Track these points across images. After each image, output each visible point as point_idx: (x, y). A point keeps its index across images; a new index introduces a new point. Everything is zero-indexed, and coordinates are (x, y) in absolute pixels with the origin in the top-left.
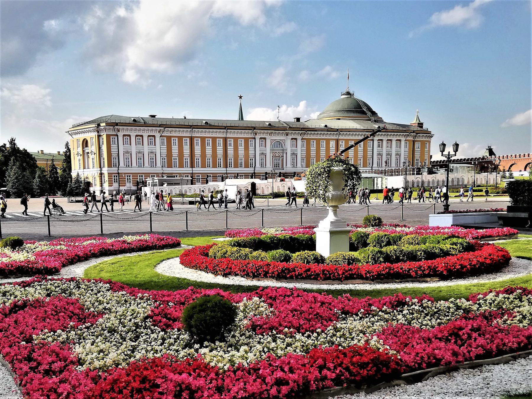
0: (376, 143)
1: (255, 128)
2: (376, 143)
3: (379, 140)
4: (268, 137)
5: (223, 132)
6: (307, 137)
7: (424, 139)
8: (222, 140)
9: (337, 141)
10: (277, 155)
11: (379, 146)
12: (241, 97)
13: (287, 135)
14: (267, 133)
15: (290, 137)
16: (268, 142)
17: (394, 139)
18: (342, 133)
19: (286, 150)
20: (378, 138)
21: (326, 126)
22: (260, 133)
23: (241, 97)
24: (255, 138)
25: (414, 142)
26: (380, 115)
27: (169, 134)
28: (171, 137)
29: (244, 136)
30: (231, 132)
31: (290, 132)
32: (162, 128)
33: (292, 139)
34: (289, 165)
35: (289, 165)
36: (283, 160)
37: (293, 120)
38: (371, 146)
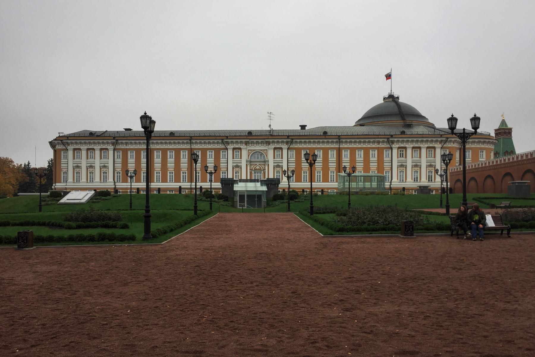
0: (395, 151)
3: (399, 148)
4: (243, 146)
5: (187, 143)
6: (296, 146)
9: (339, 151)
10: (258, 168)
13: (268, 143)
14: (241, 142)
16: (245, 153)
19: (268, 161)
20: (398, 146)
21: (325, 133)
28: (127, 150)
30: (196, 143)
31: (271, 140)
32: (114, 141)
33: (275, 149)
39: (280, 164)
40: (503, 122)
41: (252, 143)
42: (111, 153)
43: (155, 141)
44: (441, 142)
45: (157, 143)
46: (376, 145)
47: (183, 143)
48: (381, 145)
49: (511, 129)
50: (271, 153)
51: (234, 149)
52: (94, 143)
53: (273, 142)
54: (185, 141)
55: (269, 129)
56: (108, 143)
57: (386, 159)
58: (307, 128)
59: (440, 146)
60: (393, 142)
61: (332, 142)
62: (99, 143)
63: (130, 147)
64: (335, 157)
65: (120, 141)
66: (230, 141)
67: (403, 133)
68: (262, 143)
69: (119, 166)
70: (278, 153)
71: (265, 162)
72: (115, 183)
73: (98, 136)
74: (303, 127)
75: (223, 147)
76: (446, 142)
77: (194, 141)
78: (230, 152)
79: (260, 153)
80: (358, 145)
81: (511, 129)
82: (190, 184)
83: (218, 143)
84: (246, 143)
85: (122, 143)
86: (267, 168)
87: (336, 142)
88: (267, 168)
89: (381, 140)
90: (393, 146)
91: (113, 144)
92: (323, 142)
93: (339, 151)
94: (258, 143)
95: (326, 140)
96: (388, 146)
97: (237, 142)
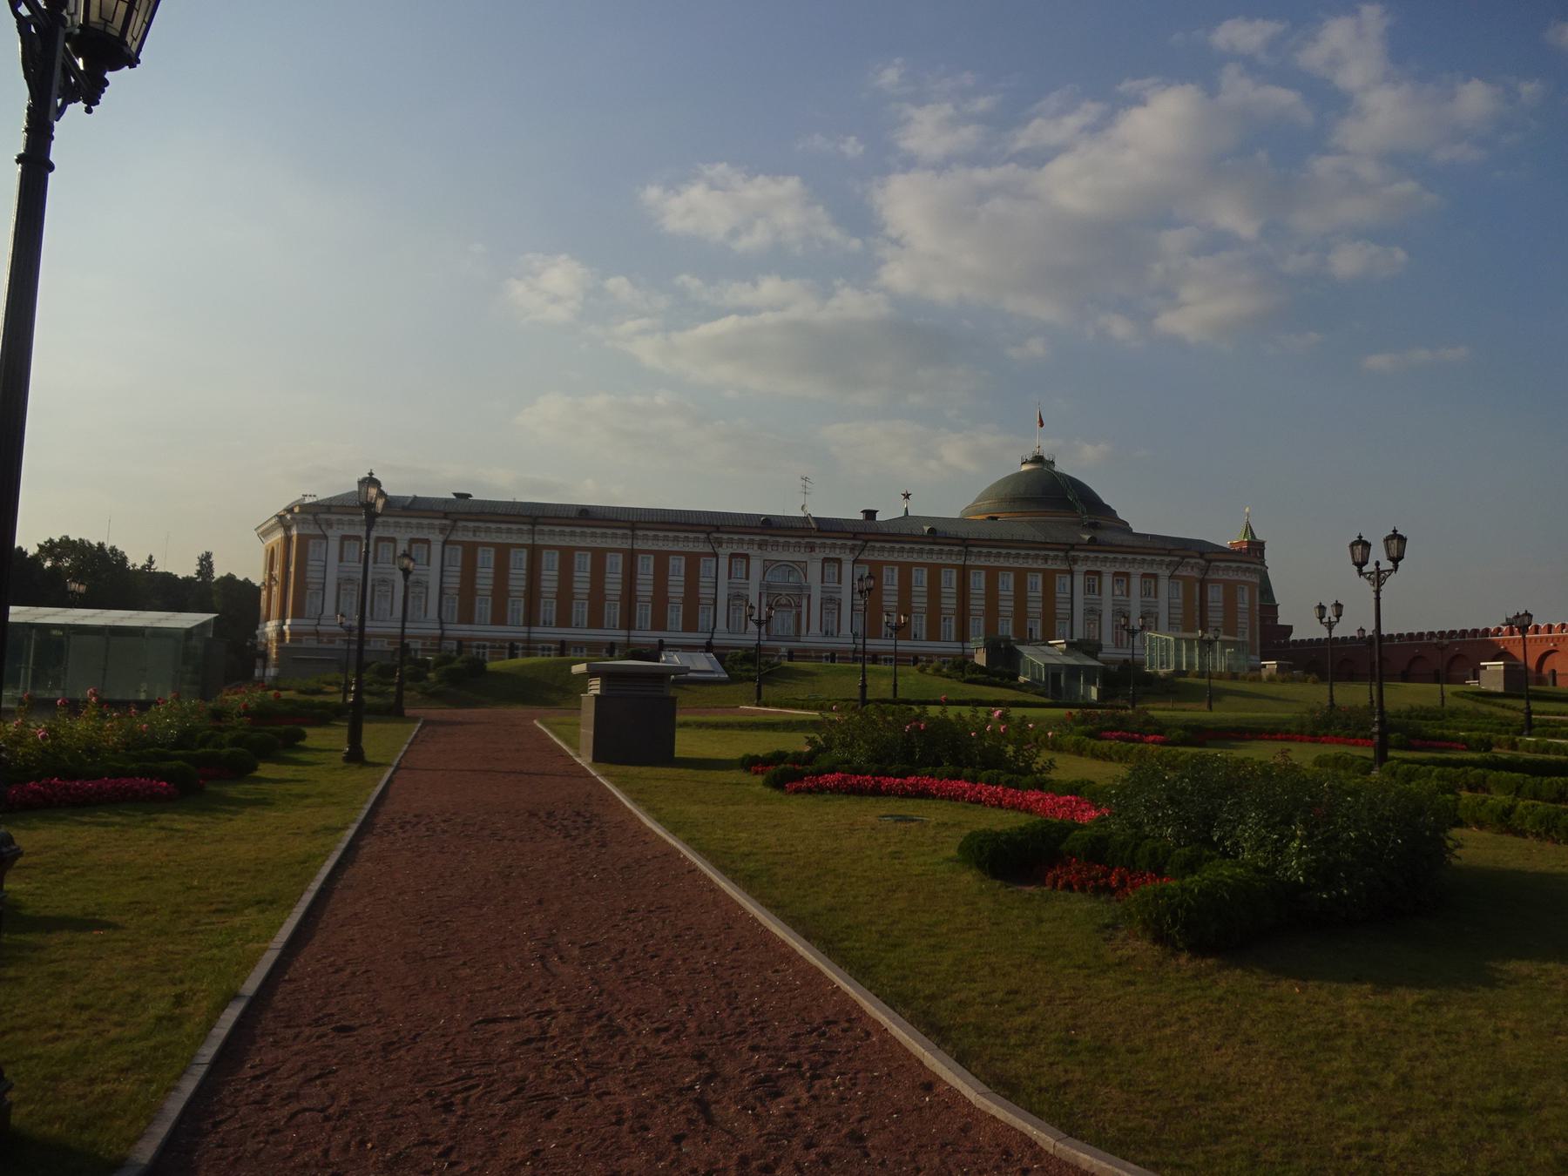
0: (1079, 581)
1: (718, 529)
2: (1079, 581)
3: (1087, 573)
4: (753, 551)
5: (624, 536)
7: (1231, 576)
8: (620, 556)
9: (964, 573)
10: (783, 601)
11: (1089, 589)
12: (907, 496)
13: (812, 549)
14: (751, 542)
15: (820, 554)
16: (756, 566)
17: (1136, 571)
18: (975, 550)
19: (809, 588)
20: (1085, 568)
22: (731, 541)
23: (907, 496)
24: (716, 555)
25: (1203, 583)
26: (1121, 516)
27: (469, 537)
28: (475, 545)
29: (655, 548)
30: (646, 537)
31: (818, 541)
32: (447, 522)
33: (825, 560)
34: (815, 628)
35: (815, 628)
36: (799, 615)
37: (861, 517)
38: (1068, 590)
39: (837, 596)
40: (1249, 529)
41: (777, 544)
42: (436, 549)
43: (546, 528)
44: (1169, 565)
45: (552, 533)
46: (1039, 565)
47: (615, 536)
48: (1051, 566)
49: (1262, 544)
50: (814, 570)
51: (732, 556)
52: (397, 525)
53: (824, 546)
54: (619, 532)
55: (802, 514)
56: (431, 527)
57: (1062, 595)
58: (879, 517)
59: (1168, 573)
60: (1075, 560)
61: (950, 553)
62: (408, 525)
63: (482, 537)
64: (954, 584)
65: (460, 524)
66: (725, 536)
67: (1093, 540)
68: (798, 545)
69: (454, 582)
70: (832, 569)
71: (801, 588)
72: (441, 623)
73: (405, 508)
74: (870, 514)
75: (708, 549)
76: (1179, 564)
77: (640, 533)
78: (724, 562)
79: (791, 567)
80: (1031, 564)
81: (1262, 544)
82: (624, 632)
83: (697, 540)
84: (761, 545)
85: (466, 529)
86: (805, 602)
87: (959, 553)
88: (805, 602)
89: (1052, 554)
90: (1076, 568)
91: (442, 530)
92: (931, 552)
93: (964, 573)
94: (787, 545)
95: (936, 548)
96: (1065, 567)
97: (741, 541)
